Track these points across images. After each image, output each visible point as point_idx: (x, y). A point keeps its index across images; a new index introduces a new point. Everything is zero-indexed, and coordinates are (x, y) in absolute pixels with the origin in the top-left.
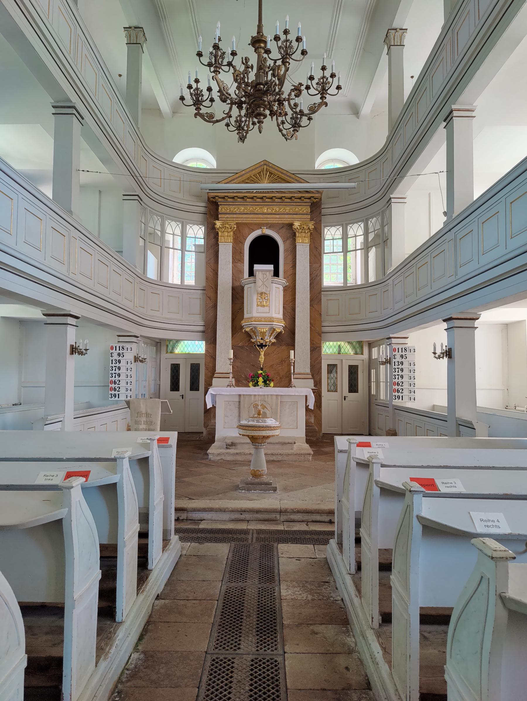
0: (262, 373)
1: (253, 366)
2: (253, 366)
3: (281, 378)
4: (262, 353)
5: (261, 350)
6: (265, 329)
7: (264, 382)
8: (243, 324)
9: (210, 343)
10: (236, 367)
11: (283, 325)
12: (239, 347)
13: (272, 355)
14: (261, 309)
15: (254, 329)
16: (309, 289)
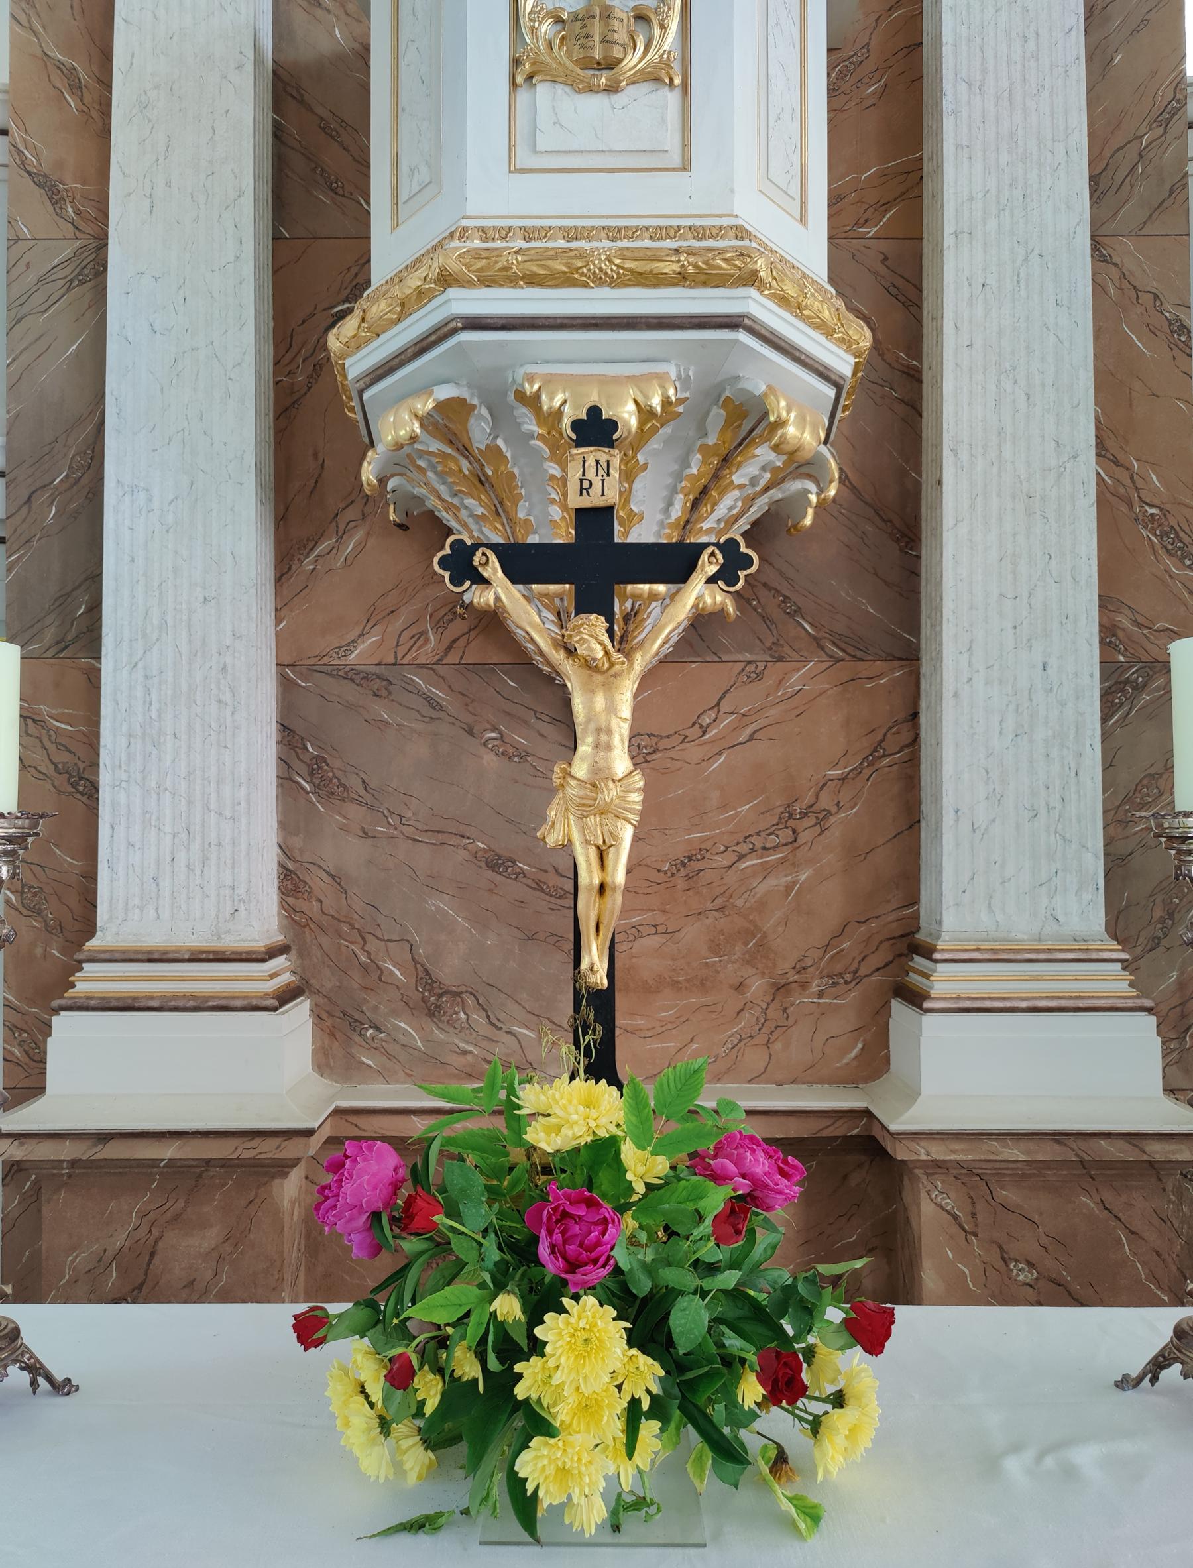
0: (603, 1151)
1: (497, 863)
2: (497, 863)
3: (780, 989)
4: (609, 711)
5: (592, 634)
6: (635, 383)
7: (689, 1396)
8: (356, 366)
9: (61, 644)
10: (318, 882)
11: (843, 364)
12: (352, 675)
13: (694, 752)
14: (571, 116)
15: (479, 431)
16: (1076, 45)
